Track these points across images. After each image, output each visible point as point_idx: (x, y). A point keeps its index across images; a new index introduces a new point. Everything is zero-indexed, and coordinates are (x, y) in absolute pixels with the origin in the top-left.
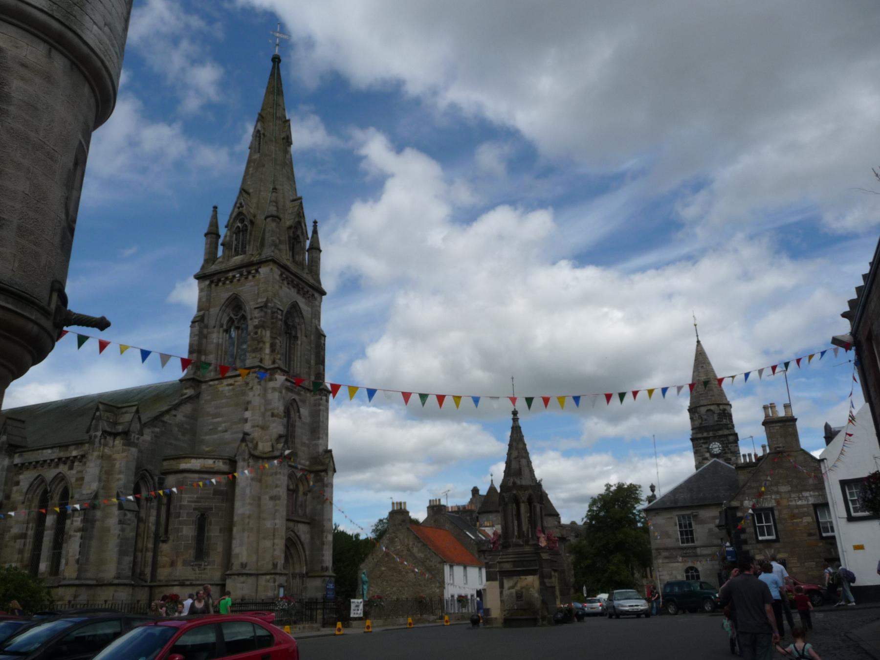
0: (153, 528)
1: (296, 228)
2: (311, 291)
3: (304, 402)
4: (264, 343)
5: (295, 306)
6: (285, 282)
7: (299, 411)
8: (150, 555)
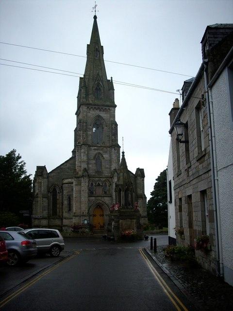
0: (61, 201)
1: (98, 86)
2: (107, 108)
4: (80, 136)
5: (99, 116)
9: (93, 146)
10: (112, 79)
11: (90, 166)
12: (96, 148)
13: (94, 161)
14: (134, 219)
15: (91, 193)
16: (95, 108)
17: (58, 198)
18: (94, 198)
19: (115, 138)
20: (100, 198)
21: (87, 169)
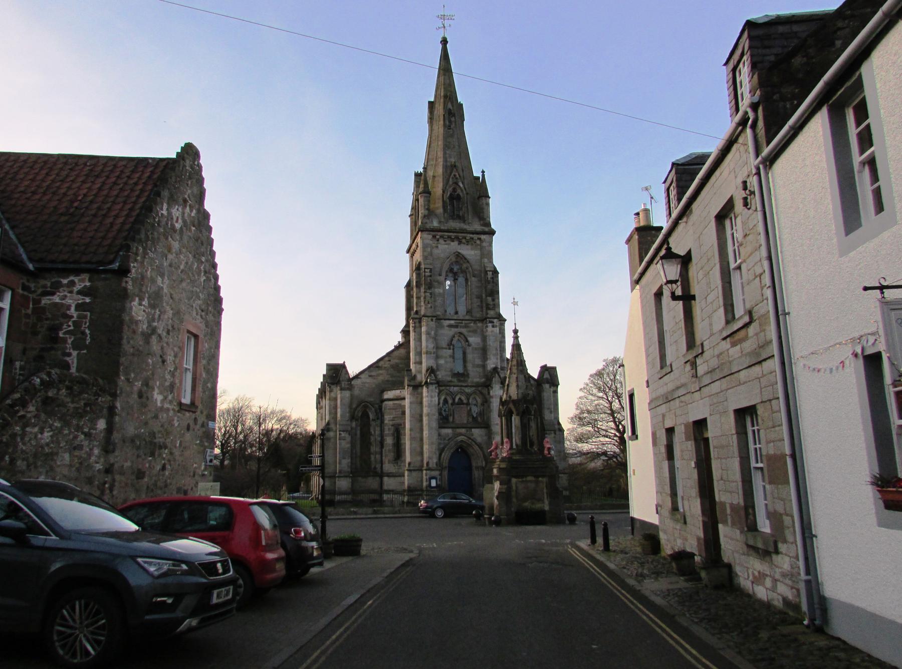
0: (379, 439)
2: (475, 237)
3: (475, 332)
5: (458, 255)
6: (441, 241)
7: (467, 341)
8: (378, 456)
10: (483, 176)
11: (442, 362)
12: (452, 322)
13: (450, 352)
14: (543, 476)
15: (444, 420)
16: (449, 237)
17: (372, 431)
19: (493, 300)
20: (463, 431)
21: (435, 367)
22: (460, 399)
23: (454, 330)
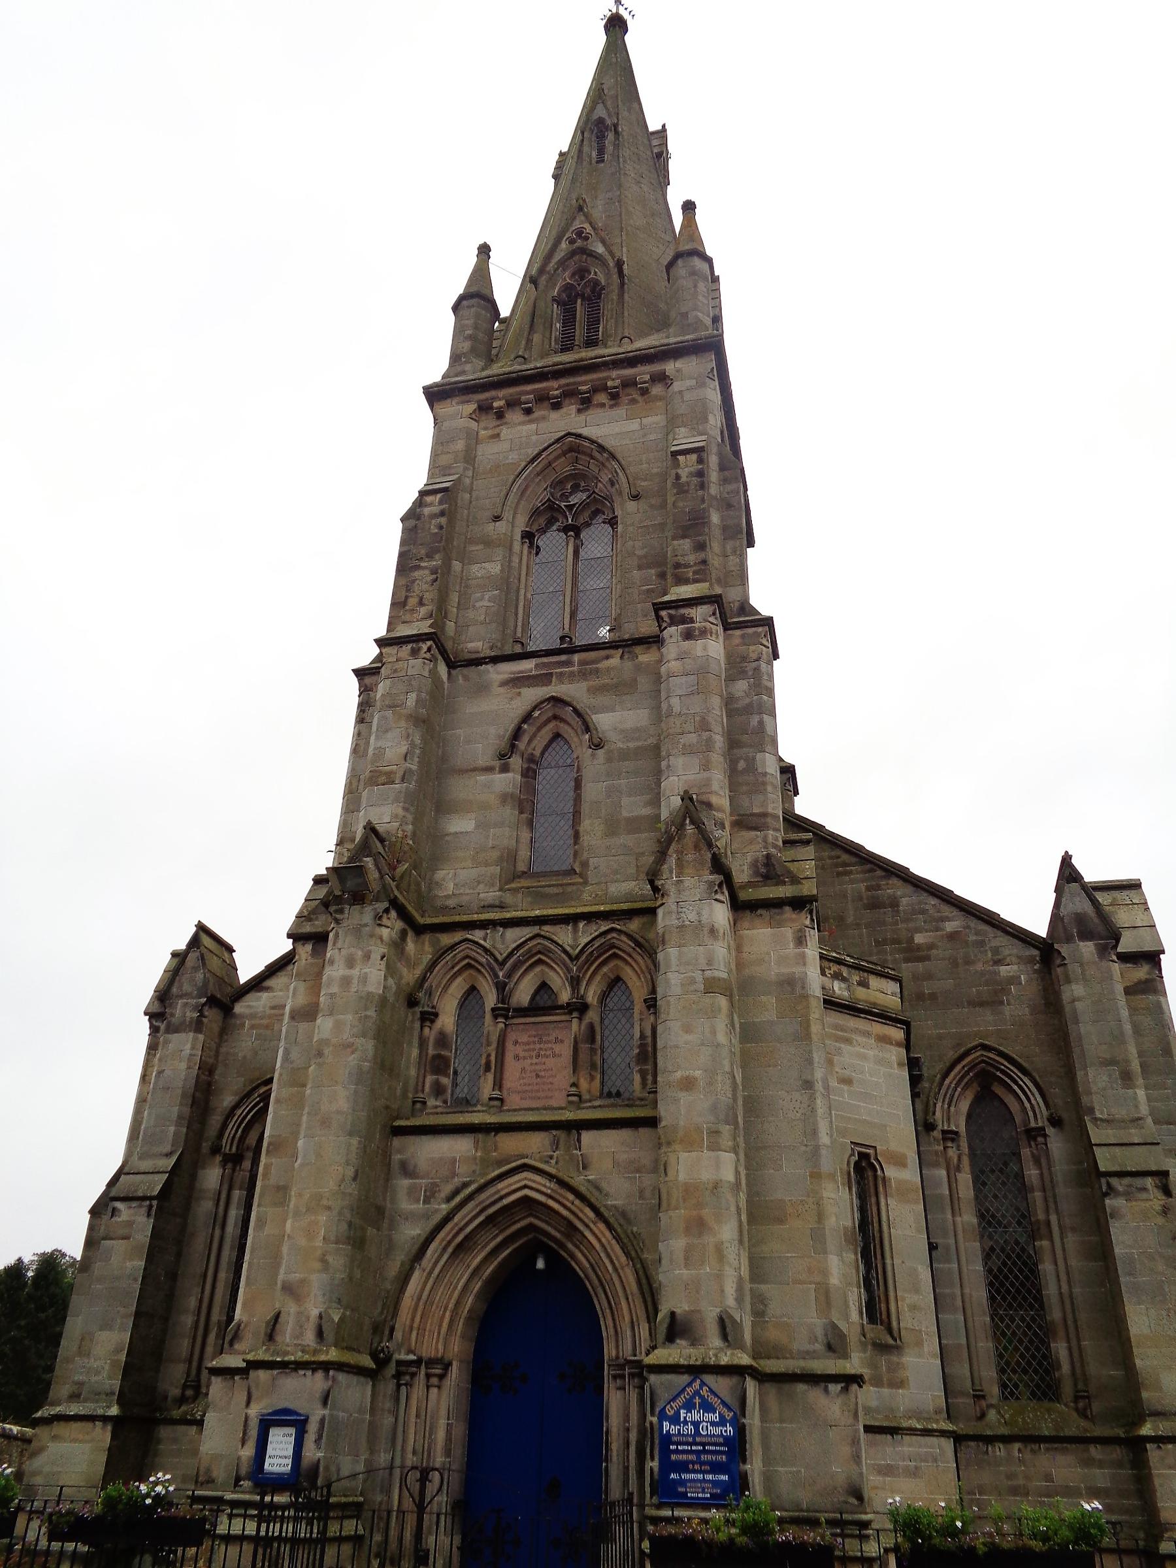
2: (643, 373)
5: (574, 446)
9: (495, 660)
12: (528, 665)
16: (542, 398)
18: (461, 1146)
20: (534, 1145)
22: (544, 986)
23: (532, 694)
